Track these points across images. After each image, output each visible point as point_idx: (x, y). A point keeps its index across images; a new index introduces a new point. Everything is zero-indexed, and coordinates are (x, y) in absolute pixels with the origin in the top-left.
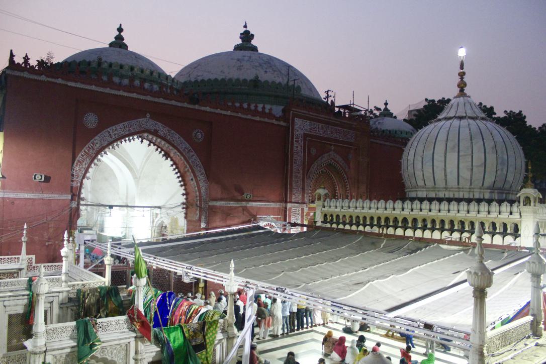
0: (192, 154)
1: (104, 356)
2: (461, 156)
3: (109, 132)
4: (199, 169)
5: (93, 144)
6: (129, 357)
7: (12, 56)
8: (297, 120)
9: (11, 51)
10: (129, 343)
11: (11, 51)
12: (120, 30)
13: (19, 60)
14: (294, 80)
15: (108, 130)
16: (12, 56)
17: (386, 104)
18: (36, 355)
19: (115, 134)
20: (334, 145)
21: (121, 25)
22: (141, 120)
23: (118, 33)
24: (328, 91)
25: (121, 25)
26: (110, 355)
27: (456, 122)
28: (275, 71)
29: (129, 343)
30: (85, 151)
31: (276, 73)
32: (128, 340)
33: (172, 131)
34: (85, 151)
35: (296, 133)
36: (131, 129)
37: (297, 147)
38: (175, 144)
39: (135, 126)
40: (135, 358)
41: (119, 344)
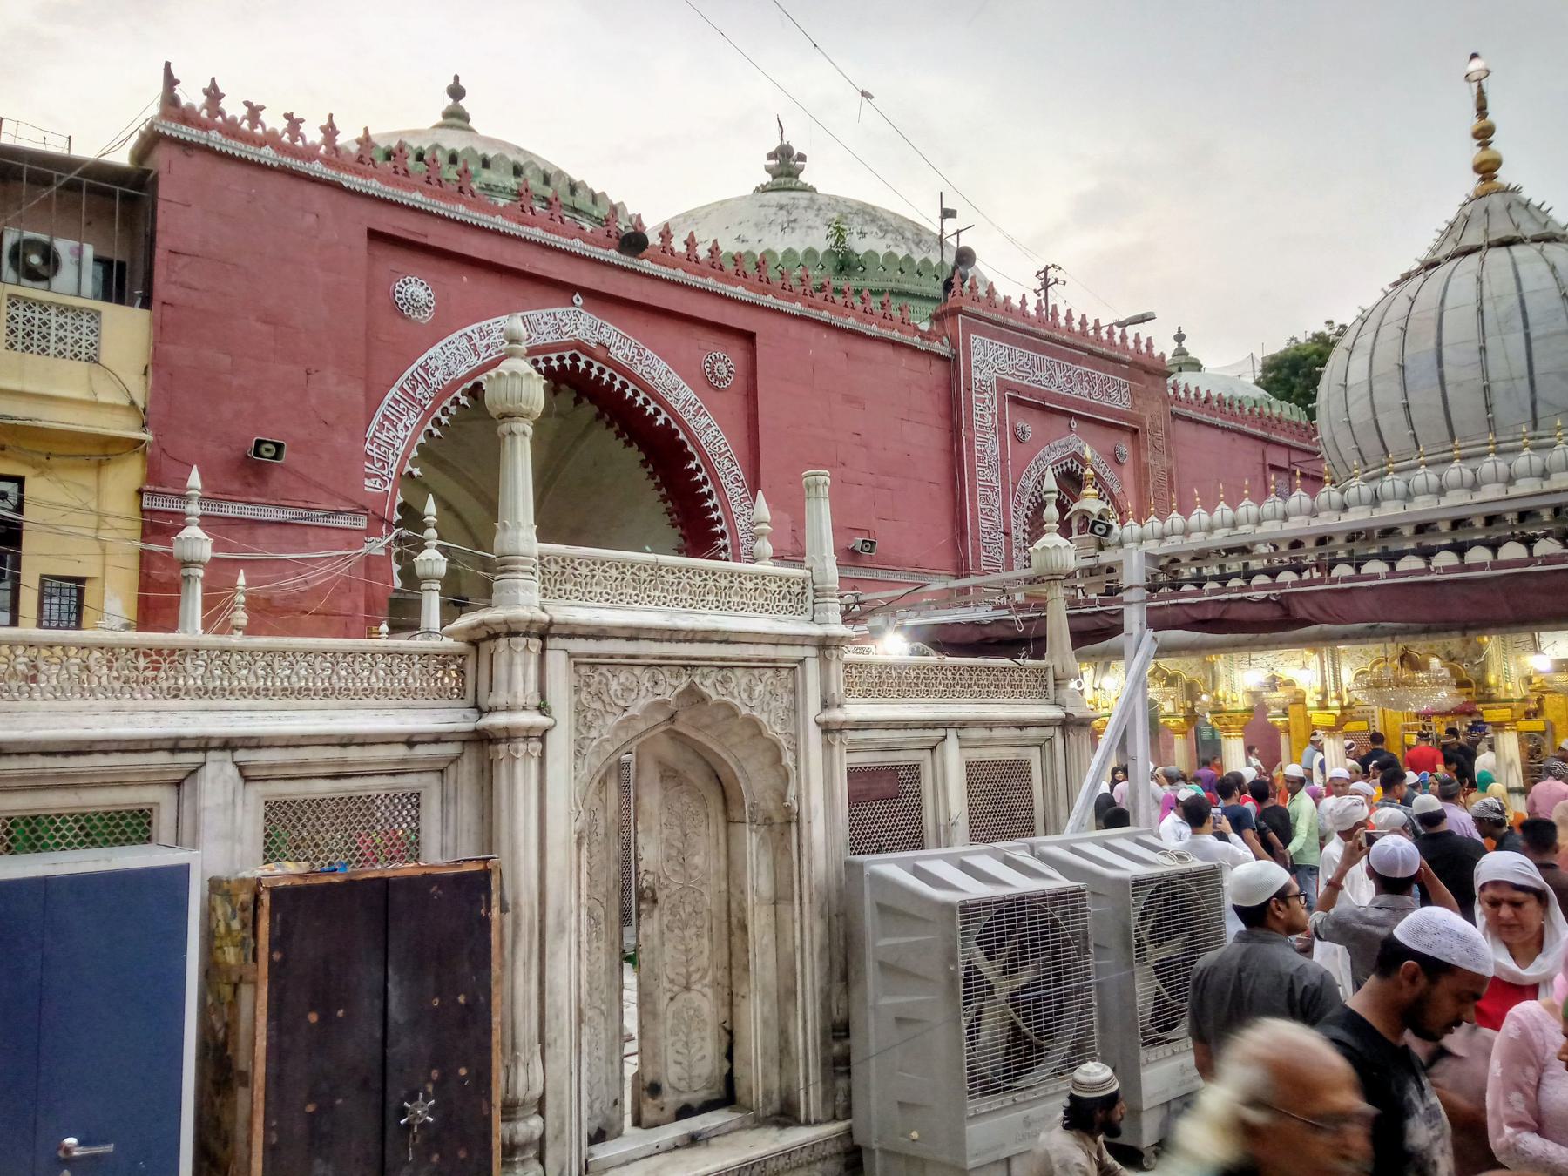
0: (705, 421)
1: (728, 699)
2: (1538, 338)
3: (470, 339)
4: (727, 464)
5: (426, 371)
6: (805, 718)
7: (170, 81)
8: (977, 341)
9: (168, 65)
10: (802, 661)
11: (168, 65)
12: (457, 92)
13: (191, 95)
14: (958, 233)
15: (468, 330)
16: (170, 81)
17: (1180, 338)
18: (513, 640)
19: (488, 346)
20: (1078, 417)
21: (457, 78)
22: (559, 311)
23: (450, 101)
24: (1047, 268)
25: (457, 78)
26: (744, 696)
27: (1498, 256)
28: (886, 232)
29: (802, 661)
30: (402, 389)
31: (889, 236)
32: (797, 652)
33: (648, 352)
34: (402, 389)
35: (976, 375)
36: (534, 335)
37: (983, 416)
38: (659, 390)
39: (544, 328)
40: (823, 717)
41: (774, 661)
